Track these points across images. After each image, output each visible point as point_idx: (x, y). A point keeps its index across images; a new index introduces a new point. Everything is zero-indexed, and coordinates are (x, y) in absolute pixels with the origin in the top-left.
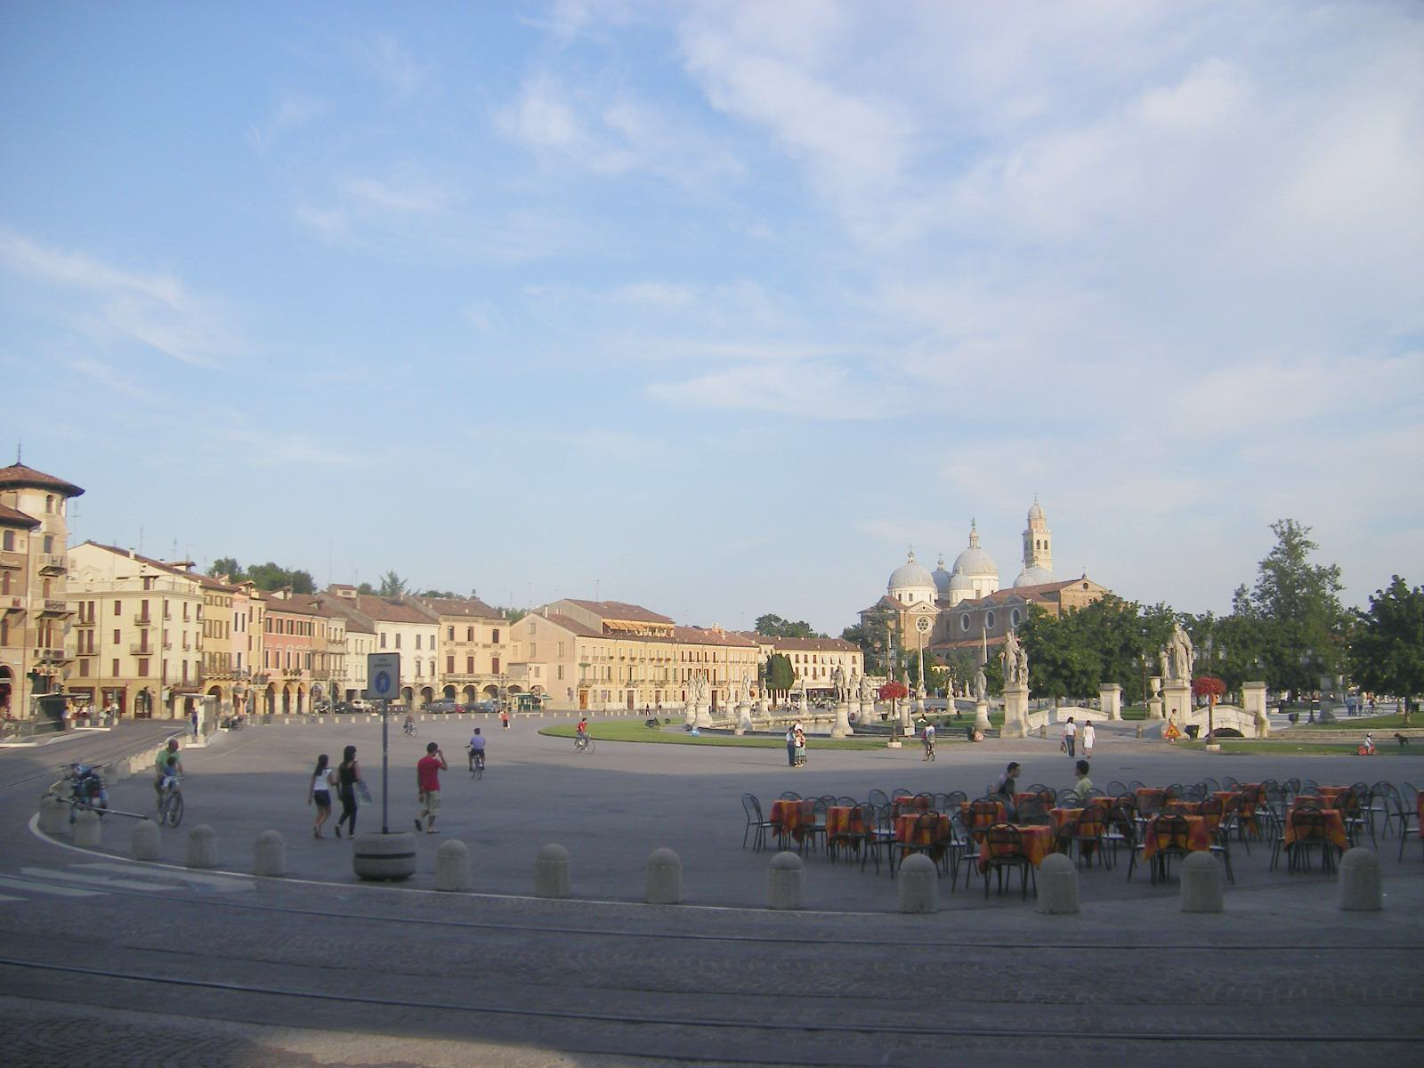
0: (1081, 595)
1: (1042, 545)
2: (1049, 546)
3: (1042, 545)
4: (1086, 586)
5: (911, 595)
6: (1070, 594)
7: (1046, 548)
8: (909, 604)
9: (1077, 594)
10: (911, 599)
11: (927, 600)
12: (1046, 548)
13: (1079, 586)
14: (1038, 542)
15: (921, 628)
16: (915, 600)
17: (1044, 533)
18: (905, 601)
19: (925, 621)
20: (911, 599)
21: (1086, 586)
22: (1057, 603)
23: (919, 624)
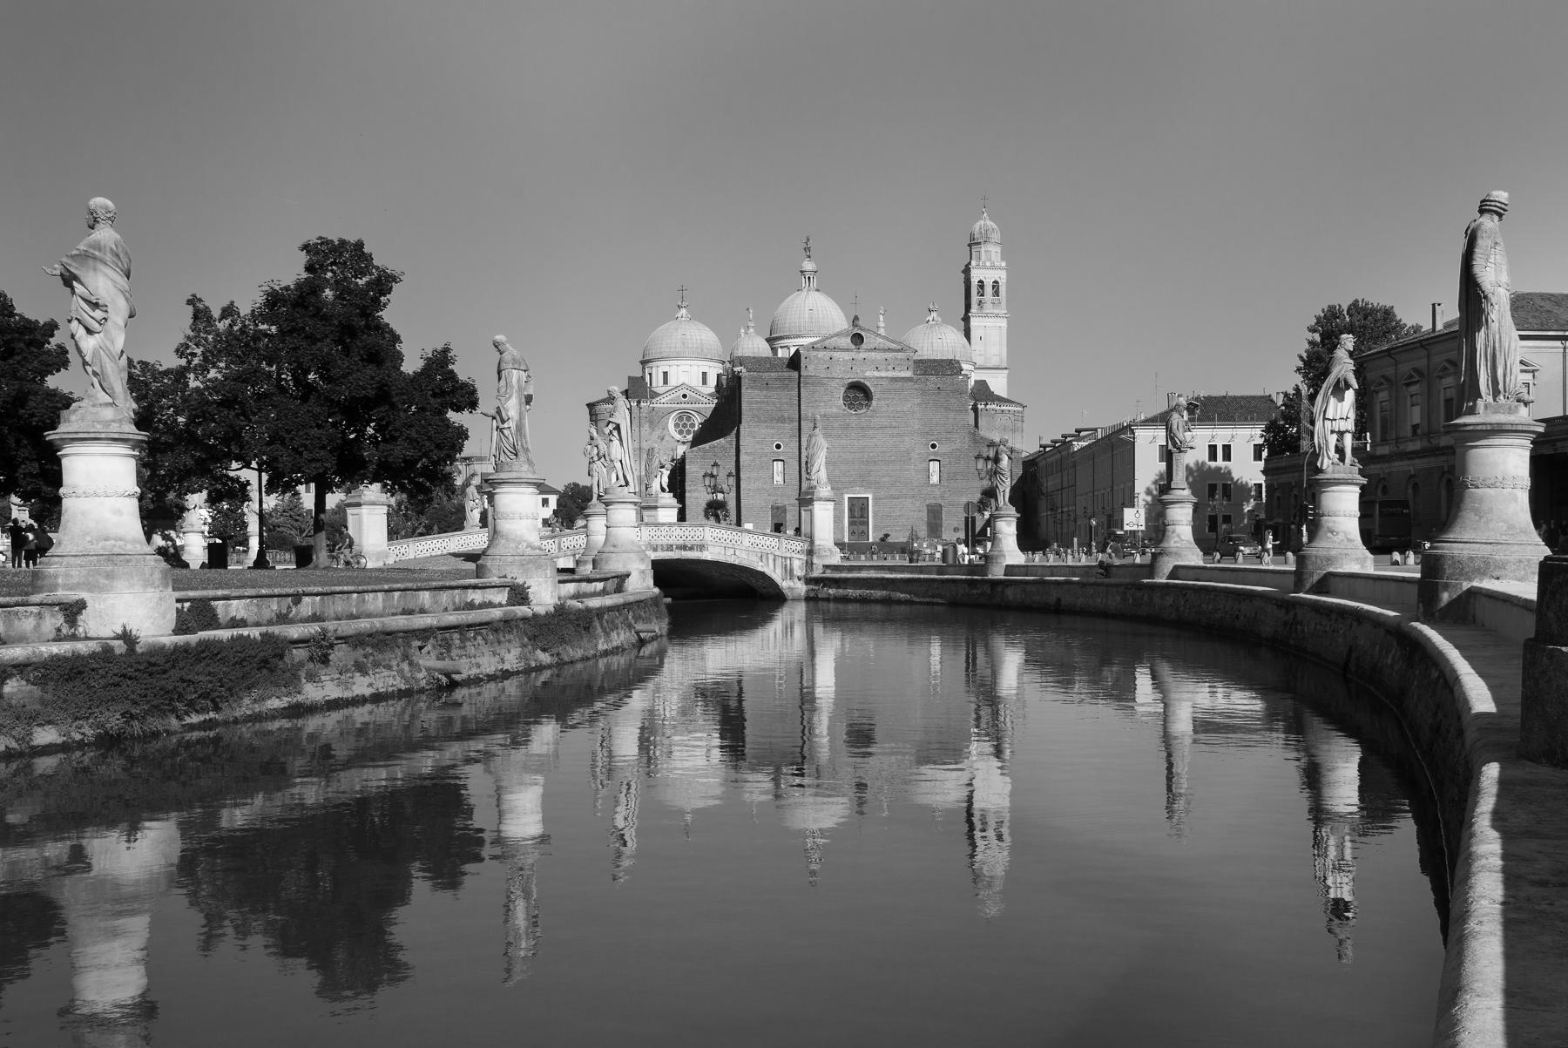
0: (846, 356)
1: (989, 290)
2: (1003, 290)
3: (989, 290)
4: (858, 339)
5: (665, 374)
6: (821, 354)
7: (996, 293)
8: (660, 390)
9: (836, 354)
10: (666, 382)
11: (696, 381)
12: (996, 293)
13: (846, 342)
14: (981, 284)
15: (681, 432)
16: (672, 382)
17: (993, 267)
18: (658, 381)
19: (689, 418)
20: (666, 382)
21: (858, 339)
22: (796, 374)
23: (677, 425)
